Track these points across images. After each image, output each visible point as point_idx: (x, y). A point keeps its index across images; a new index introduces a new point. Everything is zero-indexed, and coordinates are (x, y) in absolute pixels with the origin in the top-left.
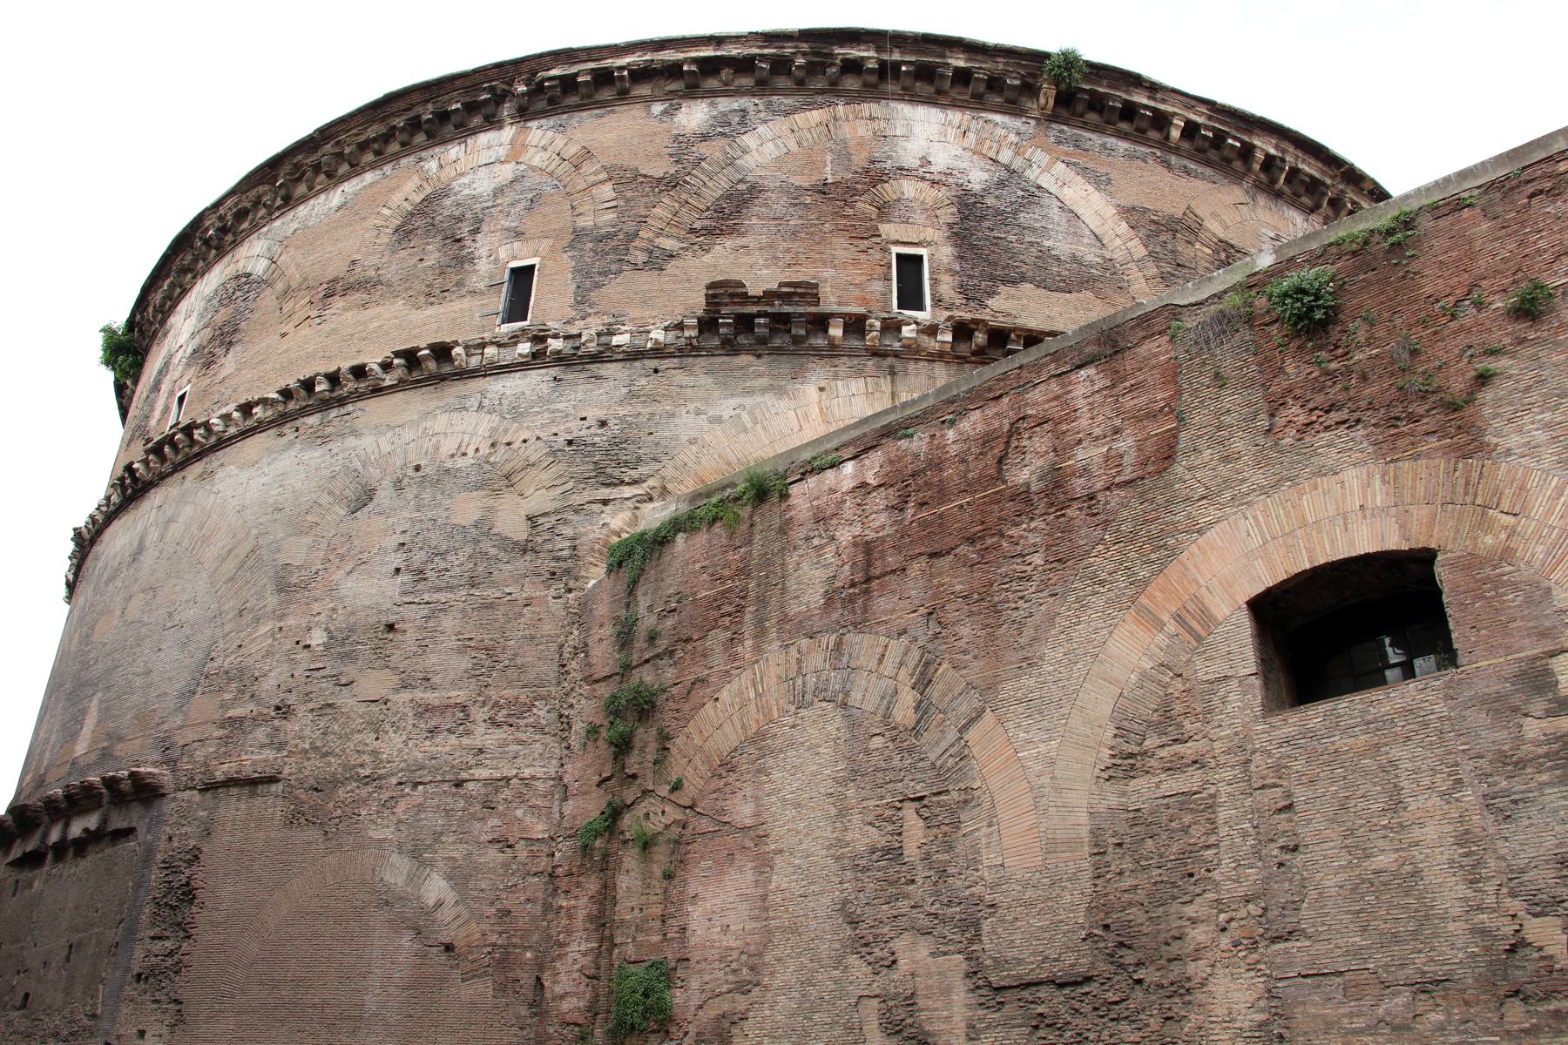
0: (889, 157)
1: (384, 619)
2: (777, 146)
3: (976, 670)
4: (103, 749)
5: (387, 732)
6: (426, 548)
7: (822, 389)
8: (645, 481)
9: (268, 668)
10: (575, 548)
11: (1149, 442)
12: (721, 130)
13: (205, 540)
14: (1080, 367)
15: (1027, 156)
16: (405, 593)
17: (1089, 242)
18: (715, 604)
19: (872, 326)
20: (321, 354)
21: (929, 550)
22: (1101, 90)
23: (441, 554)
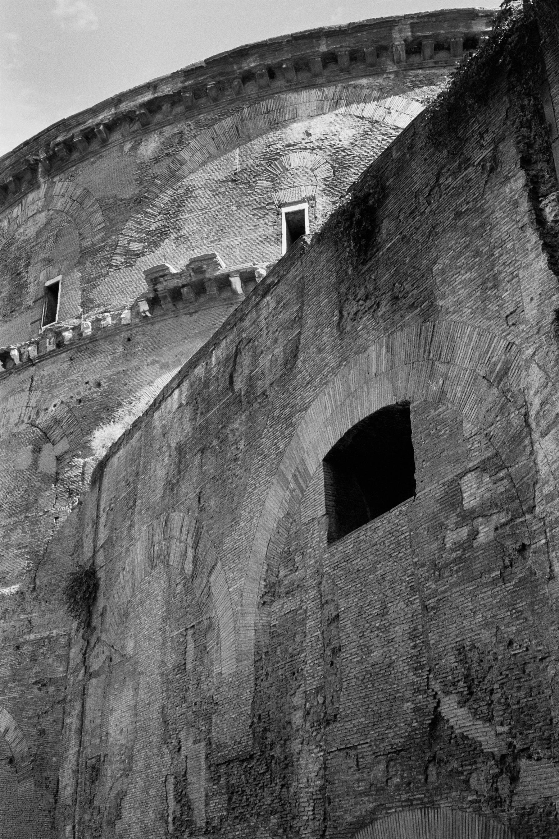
12: (166, 152)
14: (264, 296)
15: (387, 106)
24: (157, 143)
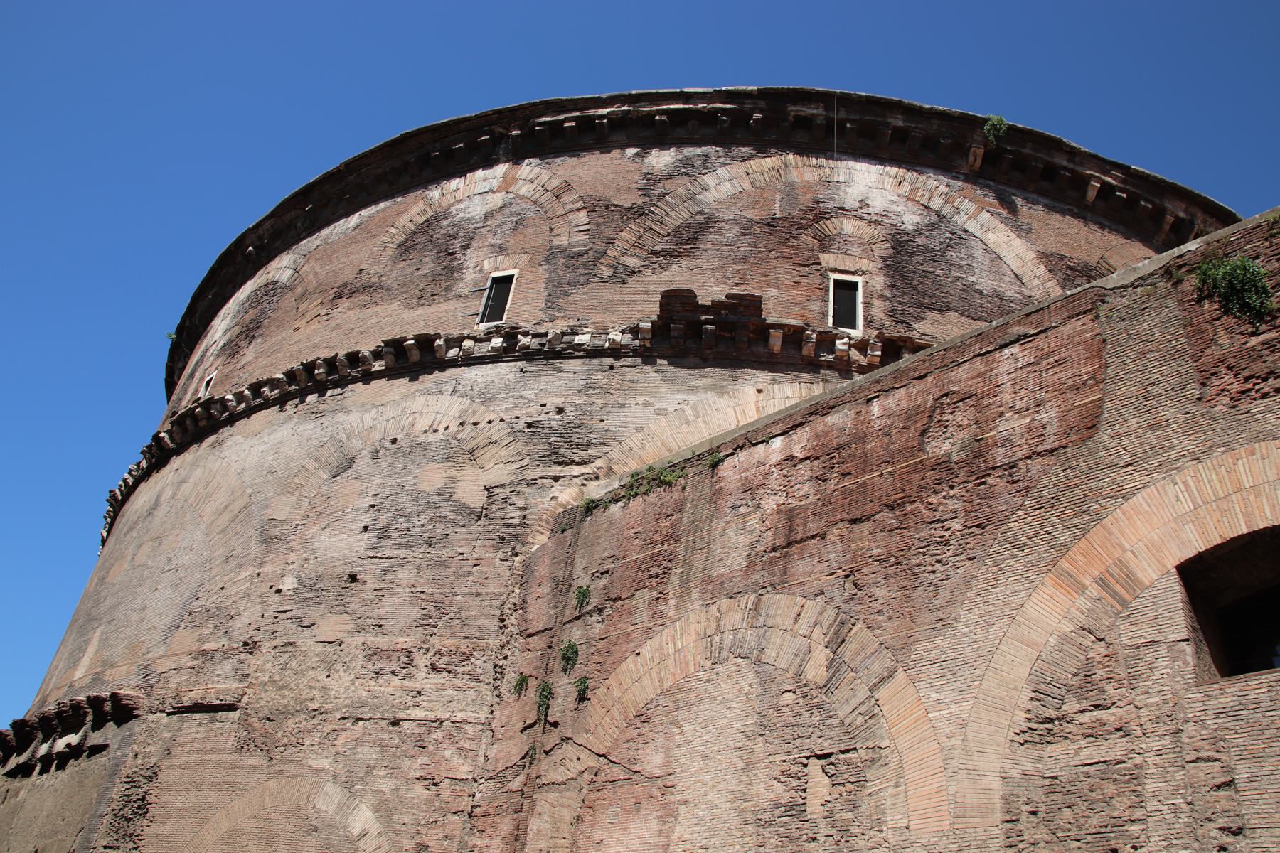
0: (831, 199)
1: (348, 570)
2: (732, 185)
3: (890, 630)
4: (96, 673)
5: (338, 671)
6: (393, 510)
7: (759, 391)
8: (593, 462)
9: (243, 608)
10: (524, 517)
11: (1072, 413)
12: (685, 170)
13: (208, 498)
15: (955, 204)
16: (370, 548)
17: (1010, 280)
18: (644, 566)
19: (809, 337)
20: (325, 345)
21: (850, 516)
22: (1026, 151)
23: (406, 516)
24: (672, 157)
